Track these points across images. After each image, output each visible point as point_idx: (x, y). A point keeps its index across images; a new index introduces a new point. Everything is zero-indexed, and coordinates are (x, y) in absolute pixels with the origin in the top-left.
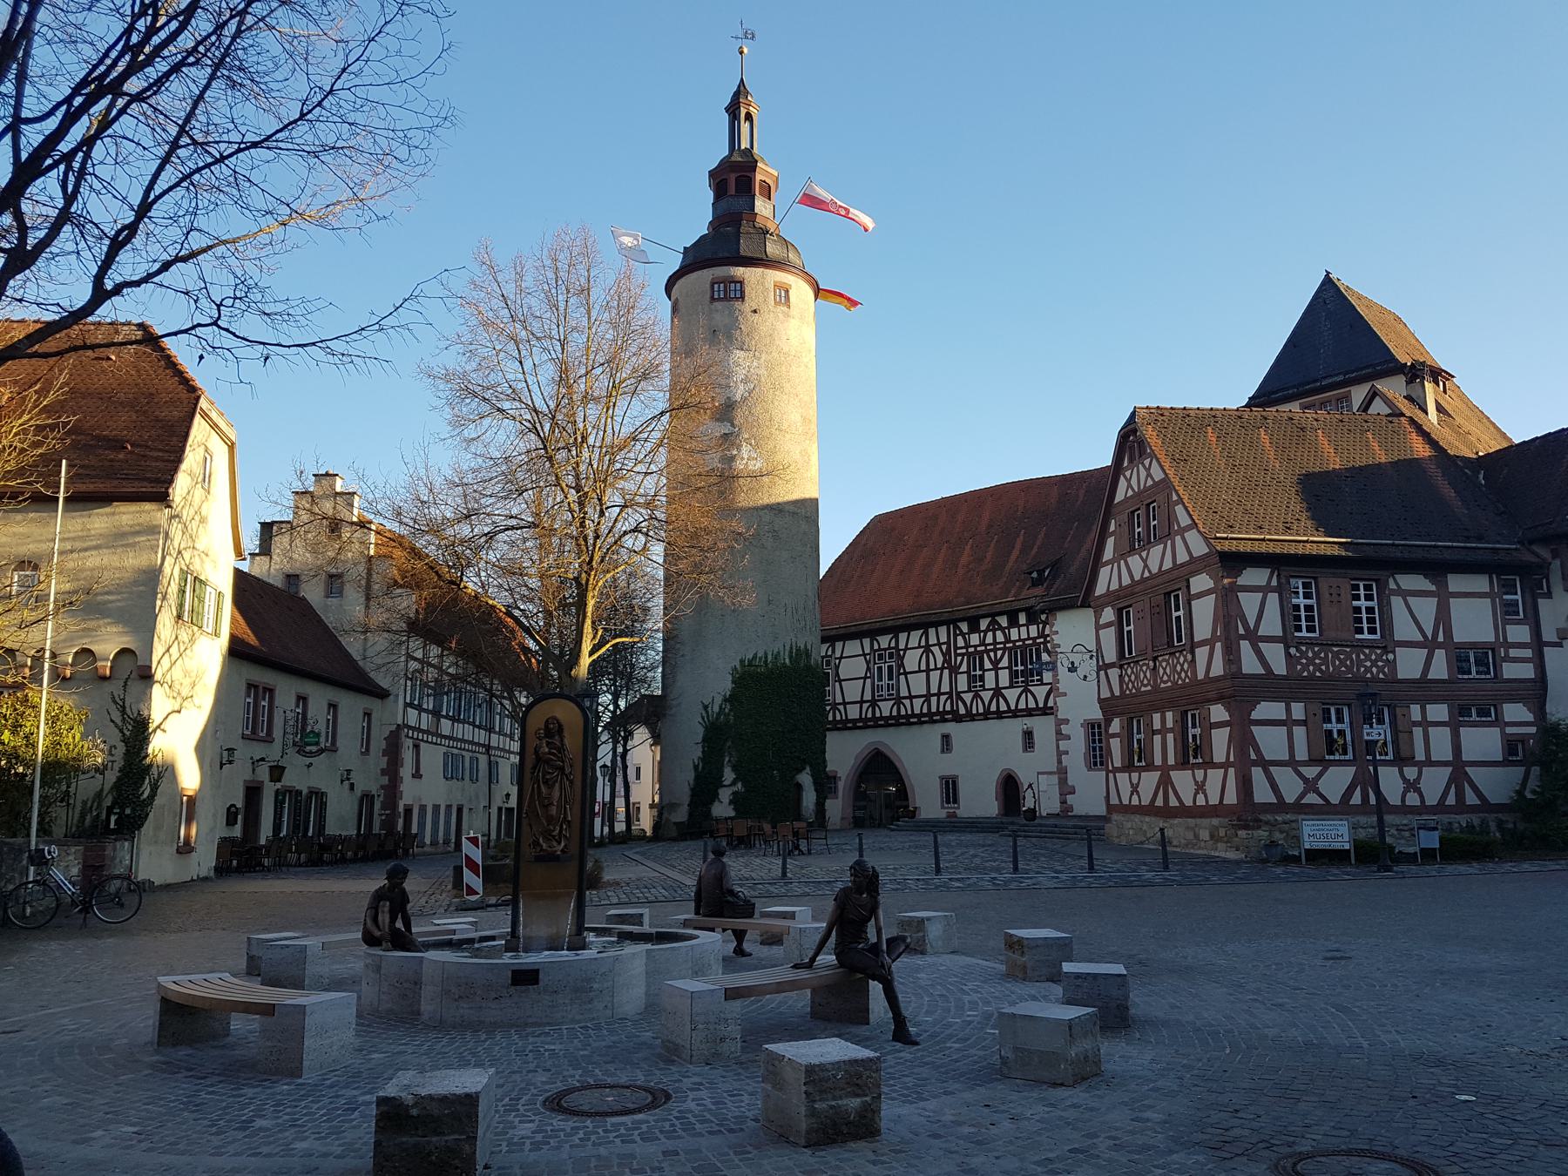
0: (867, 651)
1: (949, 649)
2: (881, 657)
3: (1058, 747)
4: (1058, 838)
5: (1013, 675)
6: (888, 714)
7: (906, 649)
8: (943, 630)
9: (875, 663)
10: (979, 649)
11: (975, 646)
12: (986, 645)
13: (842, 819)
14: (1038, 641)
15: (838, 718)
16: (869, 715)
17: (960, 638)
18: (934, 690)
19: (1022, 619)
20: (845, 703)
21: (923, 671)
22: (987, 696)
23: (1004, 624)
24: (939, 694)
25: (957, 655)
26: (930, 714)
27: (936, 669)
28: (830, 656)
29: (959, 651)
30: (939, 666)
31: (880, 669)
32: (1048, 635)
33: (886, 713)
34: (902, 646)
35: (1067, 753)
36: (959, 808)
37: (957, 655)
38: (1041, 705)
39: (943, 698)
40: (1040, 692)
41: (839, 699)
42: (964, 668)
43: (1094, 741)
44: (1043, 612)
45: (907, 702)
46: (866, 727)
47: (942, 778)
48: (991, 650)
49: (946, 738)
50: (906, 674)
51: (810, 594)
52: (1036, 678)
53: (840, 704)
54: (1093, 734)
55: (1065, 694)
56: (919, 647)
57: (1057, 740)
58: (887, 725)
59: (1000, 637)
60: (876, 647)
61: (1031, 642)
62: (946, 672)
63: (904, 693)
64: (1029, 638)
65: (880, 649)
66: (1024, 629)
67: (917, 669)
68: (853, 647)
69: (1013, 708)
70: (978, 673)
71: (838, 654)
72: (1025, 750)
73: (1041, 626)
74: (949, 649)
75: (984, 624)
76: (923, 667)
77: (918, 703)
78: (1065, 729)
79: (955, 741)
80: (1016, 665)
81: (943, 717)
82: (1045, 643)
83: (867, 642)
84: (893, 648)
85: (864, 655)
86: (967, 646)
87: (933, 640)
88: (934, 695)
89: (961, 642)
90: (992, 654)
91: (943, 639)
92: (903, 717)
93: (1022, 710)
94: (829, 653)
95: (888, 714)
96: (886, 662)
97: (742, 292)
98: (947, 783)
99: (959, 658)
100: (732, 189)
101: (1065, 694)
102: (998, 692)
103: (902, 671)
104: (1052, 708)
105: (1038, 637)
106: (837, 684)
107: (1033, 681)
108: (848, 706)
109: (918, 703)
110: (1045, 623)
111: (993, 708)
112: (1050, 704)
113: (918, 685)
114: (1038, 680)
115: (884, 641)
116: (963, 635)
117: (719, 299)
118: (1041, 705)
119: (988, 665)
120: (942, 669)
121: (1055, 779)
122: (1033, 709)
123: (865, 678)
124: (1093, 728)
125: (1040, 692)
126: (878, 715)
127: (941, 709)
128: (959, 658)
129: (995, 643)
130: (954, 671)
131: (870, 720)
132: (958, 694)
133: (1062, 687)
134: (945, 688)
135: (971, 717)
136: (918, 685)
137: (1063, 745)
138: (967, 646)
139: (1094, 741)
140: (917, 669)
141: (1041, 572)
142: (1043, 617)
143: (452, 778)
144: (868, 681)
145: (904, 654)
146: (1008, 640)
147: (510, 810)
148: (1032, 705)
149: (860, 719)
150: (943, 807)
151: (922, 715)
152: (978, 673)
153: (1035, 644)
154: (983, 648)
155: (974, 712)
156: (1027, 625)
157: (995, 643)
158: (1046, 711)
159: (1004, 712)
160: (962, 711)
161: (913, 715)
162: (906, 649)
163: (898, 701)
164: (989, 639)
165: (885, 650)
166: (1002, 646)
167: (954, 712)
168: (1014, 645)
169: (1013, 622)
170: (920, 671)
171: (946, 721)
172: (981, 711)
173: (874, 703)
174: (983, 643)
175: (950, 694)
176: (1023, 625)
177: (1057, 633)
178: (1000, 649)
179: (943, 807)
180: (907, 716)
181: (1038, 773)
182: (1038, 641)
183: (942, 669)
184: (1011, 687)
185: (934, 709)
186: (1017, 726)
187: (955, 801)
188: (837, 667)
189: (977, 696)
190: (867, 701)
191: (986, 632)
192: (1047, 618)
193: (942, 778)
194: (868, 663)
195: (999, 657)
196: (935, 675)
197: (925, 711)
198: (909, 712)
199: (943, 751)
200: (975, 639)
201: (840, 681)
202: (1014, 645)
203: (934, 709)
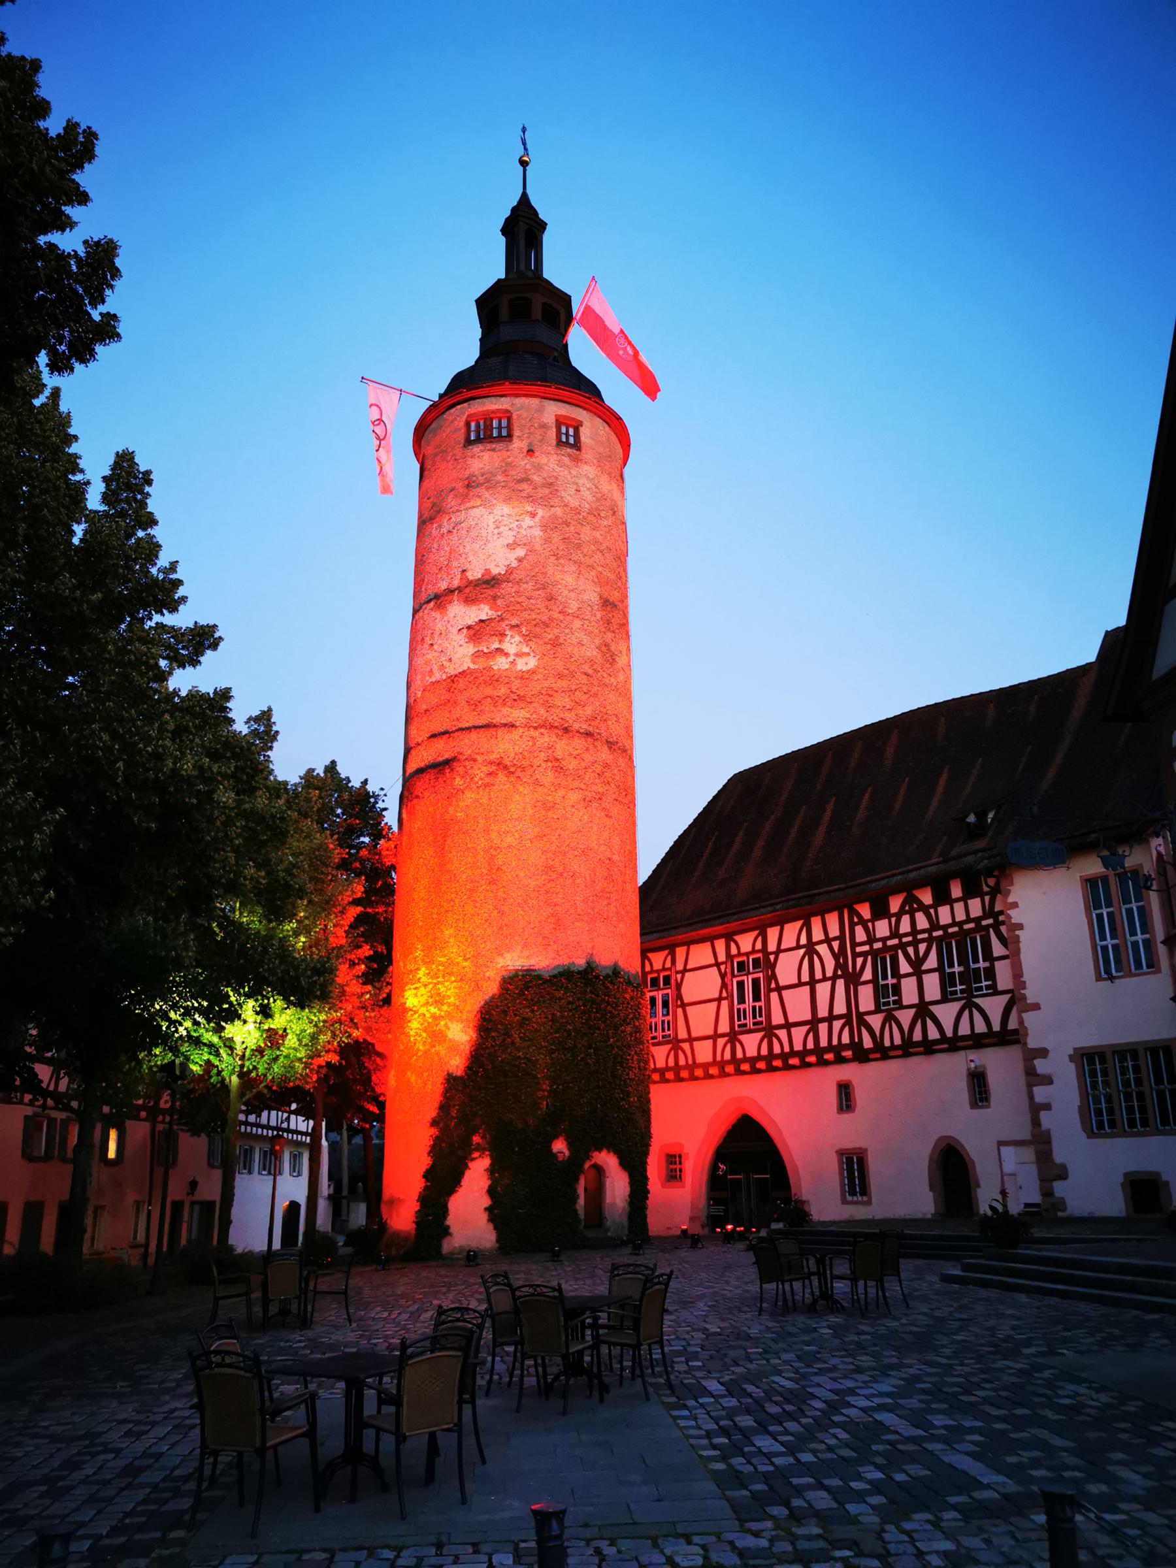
0: (722, 958)
1: (842, 946)
2: (742, 966)
3: (1031, 1097)
4: (1084, 1298)
5: (947, 981)
6: (755, 1054)
7: (779, 951)
8: (833, 921)
9: (733, 976)
10: (890, 943)
11: (884, 940)
12: (900, 936)
13: (692, 1219)
14: (984, 923)
15: (682, 1062)
16: (727, 1056)
17: (859, 930)
18: (823, 1012)
19: (956, 891)
20: (691, 1040)
21: (805, 984)
22: (905, 1017)
23: (927, 898)
24: (831, 1018)
25: (855, 955)
26: (818, 1051)
27: (825, 979)
28: (670, 969)
29: (858, 949)
30: (829, 973)
31: (741, 985)
32: (1001, 913)
33: (751, 1052)
34: (772, 947)
35: (1047, 1107)
36: (869, 1203)
37: (855, 955)
38: (996, 1027)
39: (837, 1025)
40: (994, 1006)
41: (682, 1034)
42: (867, 975)
43: (1094, 1085)
44: (989, 873)
45: (782, 1033)
46: (723, 1074)
47: (841, 1153)
48: (909, 944)
49: (845, 1091)
50: (779, 989)
51: (615, 857)
52: (984, 984)
53: (684, 1041)
54: (1093, 1074)
55: (1036, 1007)
56: (798, 947)
57: (1030, 1086)
58: (755, 1071)
59: (922, 922)
60: (734, 951)
61: (972, 925)
62: (840, 984)
63: (777, 1019)
64: (969, 920)
65: (739, 954)
66: (959, 908)
67: (796, 981)
68: (701, 954)
69: (949, 1033)
70: (891, 981)
71: (680, 967)
72: (974, 1105)
73: (987, 898)
74: (842, 946)
75: (895, 904)
76: (805, 977)
77: (799, 1033)
78: (1041, 1066)
79: (860, 1095)
80: (951, 965)
81: (837, 1055)
82: (996, 926)
83: (720, 945)
84: (758, 951)
85: (717, 964)
86: (871, 939)
87: (818, 935)
88: (823, 1020)
89: (861, 935)
90: (910, 950)
91: (834, 931)
92: (777, 1057)
93: (964, 1038)
94: (668, 965)
95: (755, 1054)
96: (749, 973)
97: (510, 428)
98: (850, 1161)
99: (860, 961)
100: (504, 311)
101: (1036, 1007)
102: (923, 1010)
103: (773, 985)
104: (1015, 1032)
105: (984, 917)
106: (680, 1011)
107: (980, 989)
108: (696, 1044)
109: (799, 1033)
110: (995, 891)
111: (917, 1036)
112: (1012, 1024)
113: (798, 1005)
114: (987, 987)
115: (746, 942)
116: (863, 923)
117: (478, 440)
118: (996, 1027)
119: (905, 967)
120: (834, 979)
121: (1029, 1154)
122: (982, 1035)
123: (719, 1000)
124: (1091, 1062)
125: (994, 1006)
126: (739, 1055)
127: (835, 1042)
128: (860, 961)
129: (914, 931)
130: (853, 980)
131: (728, 1062)
132: (860, 1016)
133: (1031, 994)
134: (840, 1008)
135: (882, 1052)
136: (798, 1005)
137: (1041, 1093)
138: (871, 939)
139: (1094, 1085)
140: (796, 981)
141: (981, 816)
142: (992, 882)
143: (47, 1158)
144: (724, 1004)
145: (776, 959)
146: (934, 925)
147: (208, 1206)
148: (980, 1027)
149: (715, 1062)
150: (844, 1201)
151: (805, 1052)
152: (891, 981)
153: (979, 928)
154: (895, 941)
155: (887, 1043)
156: (964, 899)
157: (914, 931)
158: (1007, 1037)
159: (936, 1042)
160: (868, 1043)
161: (793, 1053)
162: (779, 951)
163: (769, 1031)
164: (905, 926)
165: (747, 954)
166: (926, 935)
167: (856, 1046)
168: (945, 931)
169: (943, 897)
170: (800, 984)
171: (840, 1060)
172: (898, 1040)
173: (733, 1037)
174: (895, 933)
175: (847, 1017)
176: (958, 900)
177: (1015, 905)
178: (923, 941)
179: (844, 1201)
180: (784, 1056)
181: (1001, 1144)
182: (984, 923)
183: (834, 979)
184: (945, 999)
185: (824, 1043)
186: (956, 1065)
187: (865, 1190)
188: (679, 986)
189: (890, 1018)
190: (723, 1035)
191: (899, 916)
192: (998, 884)
193: (841, 1153)
194: (723, 976)
195: (921, 953)
196: (823, 990)
197: (810, 1045)
198: (787, 1049)
199: (841, 1110)
200: (882, 928)
201: (684, 1006)
202: (945, 931)
203: (824, 1043)
